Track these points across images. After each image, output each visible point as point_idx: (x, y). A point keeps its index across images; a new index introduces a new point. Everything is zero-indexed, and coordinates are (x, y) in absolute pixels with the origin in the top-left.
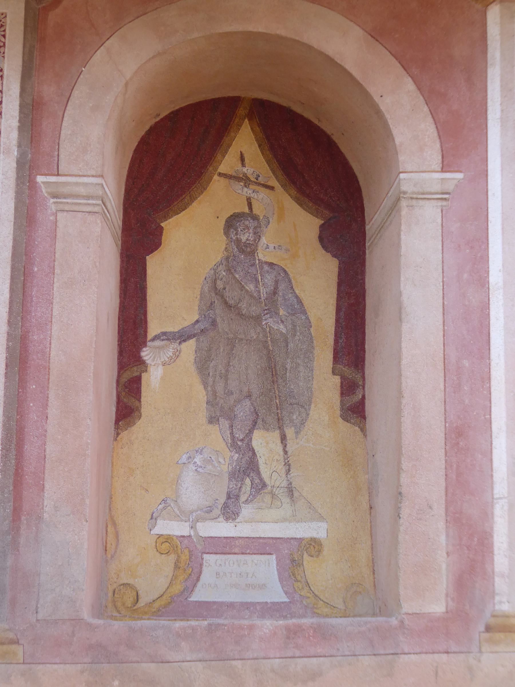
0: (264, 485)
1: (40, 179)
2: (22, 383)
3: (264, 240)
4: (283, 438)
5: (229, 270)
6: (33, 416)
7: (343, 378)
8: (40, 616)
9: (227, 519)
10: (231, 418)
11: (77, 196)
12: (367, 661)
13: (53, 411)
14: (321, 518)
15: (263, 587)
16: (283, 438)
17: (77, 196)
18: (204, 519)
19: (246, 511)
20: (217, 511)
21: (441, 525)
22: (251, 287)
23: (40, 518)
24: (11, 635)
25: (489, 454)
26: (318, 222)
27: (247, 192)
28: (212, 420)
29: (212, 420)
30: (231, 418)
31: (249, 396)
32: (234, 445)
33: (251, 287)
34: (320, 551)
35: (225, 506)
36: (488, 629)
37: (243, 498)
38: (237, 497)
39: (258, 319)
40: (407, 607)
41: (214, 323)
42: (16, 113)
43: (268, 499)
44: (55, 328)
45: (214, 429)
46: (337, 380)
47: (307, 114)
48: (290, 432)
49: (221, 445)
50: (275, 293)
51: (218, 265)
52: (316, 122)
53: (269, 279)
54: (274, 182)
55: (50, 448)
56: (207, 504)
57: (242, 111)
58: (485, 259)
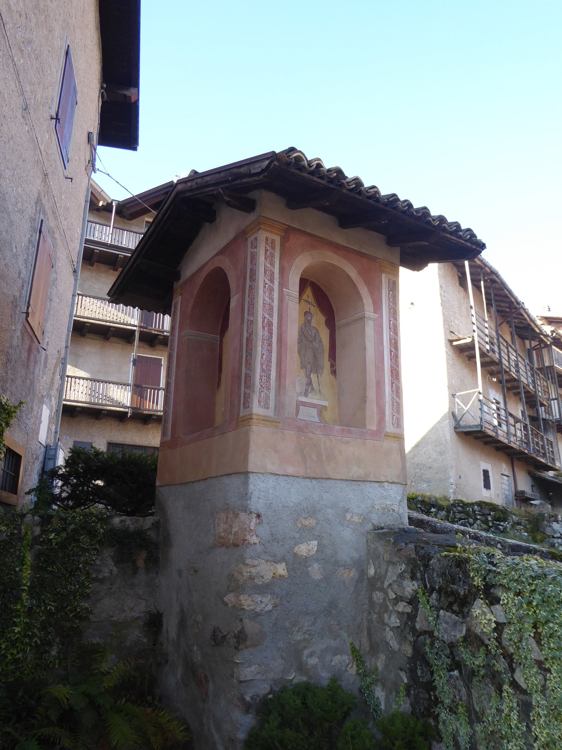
0: (314, 389)
1: (284, 289)
2: (281, 347)
3: (313, 320)
4: (318, 376)
5: (305, 326)
6: (283, 358)
7: (331, 363)
8: (285, 416)
9: (305, 397)
10: (306, 368)
11: (292, 297)
12: (359, 440)
13: (288, 357)
14: (327, 401)
15: (313, 417)
16: (318, 376)
17: (292, 297)
18: (300, 396)
19: (310, 395)
20: (303, 394)
21: (375, 407)
22: (310, 332)
23: (285, 387)
24: (278, 420)
25: (384, 389)
26: (325, 319)
27: (309, 306)
28: (302, 368)
29: (302, 368)
30: (306, 368)
31: (310, 363)
32: (307, 377)
33: (310, 332)
34: (327, 409)
35: (305, 393)
36: (385, 436)
37: (309, 392)
38: (308, 391)
39: (312, 342)
40: (368, 427)
41: (302, 340)
42: (278, 269)
43: (315, 392)
44: (288, 333)
45: (302, 371)
46: (330, 363)
47: (324, 289)
48: (319, 375)
49: (304, 376)
50: (315, 335)
51: (303, 324)
52: (325, 292)
53: (314, 331)
54: (315, 305)
55: (287, 368)
56: (300, 391)
57: (308, 283)
58: (383, 338)
